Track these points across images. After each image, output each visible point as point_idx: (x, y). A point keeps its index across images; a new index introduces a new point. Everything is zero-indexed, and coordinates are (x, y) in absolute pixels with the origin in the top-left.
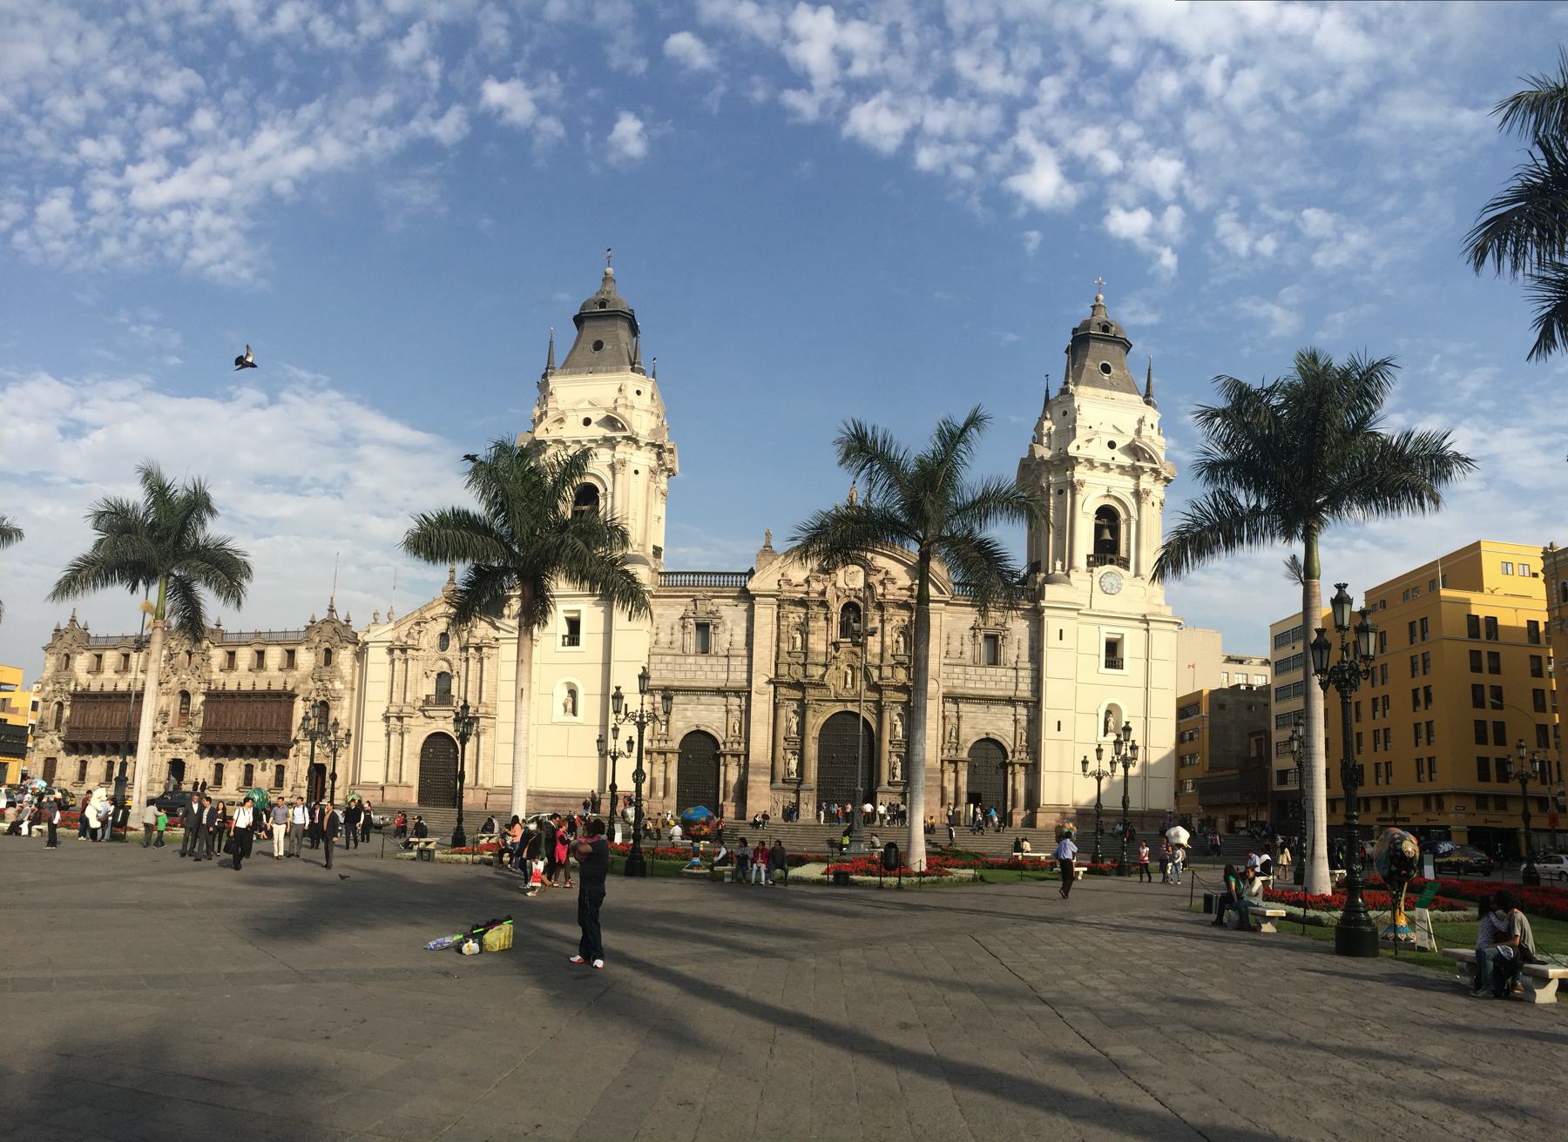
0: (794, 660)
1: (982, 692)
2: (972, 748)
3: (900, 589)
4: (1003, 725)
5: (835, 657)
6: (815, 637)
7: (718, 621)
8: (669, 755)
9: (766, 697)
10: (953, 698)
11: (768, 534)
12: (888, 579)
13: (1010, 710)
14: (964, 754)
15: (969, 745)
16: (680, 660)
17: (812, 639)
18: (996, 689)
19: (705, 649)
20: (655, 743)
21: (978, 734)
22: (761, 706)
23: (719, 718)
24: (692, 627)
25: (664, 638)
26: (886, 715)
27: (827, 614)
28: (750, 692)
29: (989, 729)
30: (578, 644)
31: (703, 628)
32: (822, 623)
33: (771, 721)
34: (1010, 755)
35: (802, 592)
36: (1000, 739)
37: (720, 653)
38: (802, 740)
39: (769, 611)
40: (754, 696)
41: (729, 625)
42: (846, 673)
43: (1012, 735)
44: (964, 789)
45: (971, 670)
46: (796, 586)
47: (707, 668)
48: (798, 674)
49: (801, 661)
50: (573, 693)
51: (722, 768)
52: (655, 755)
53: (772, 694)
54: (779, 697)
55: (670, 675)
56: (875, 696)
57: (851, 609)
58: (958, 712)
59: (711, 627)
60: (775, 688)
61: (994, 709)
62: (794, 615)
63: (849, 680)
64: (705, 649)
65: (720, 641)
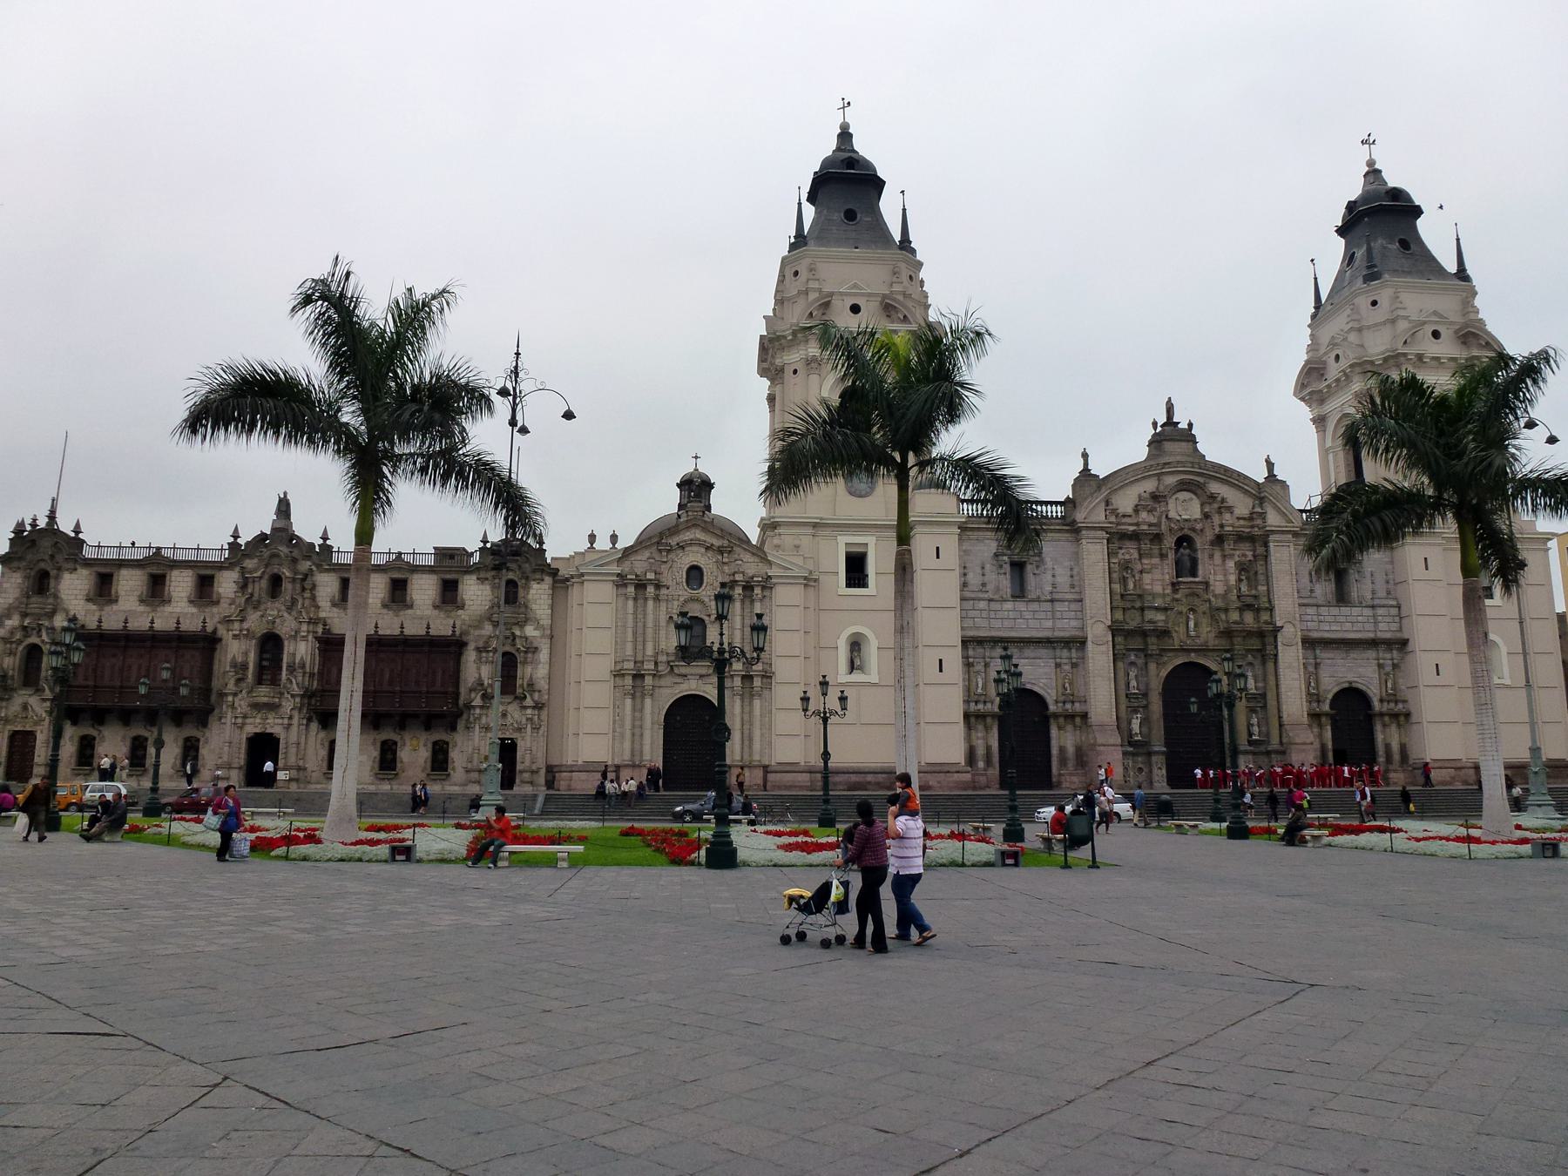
0: (1128, 605)
2: (1334, 697)
3: (1238, 518)
4: (1363, 672)
5: (1177, 600)
6: (1149, 576)
7: (1037, 558)
8: (989, 720)
9: (1103, 648)
10: (1309, 643)
11: (1085, 456)
12: (1224, 507)
13: (1371, 654)
14: (1326, 707)
15: (1330, 696)
16: (994, 606)
19: (1020, 592)
20: (972, 704)
21: (1337, 685)
22: (1099, 657)
23: (1046, 674)
24: (1007, 567)
25: (974, 579)
27: (1161, 549)
29: (1350, 677)
32: (1156, 561)
33: (1112, 675)
34: (1376, 705)
36: (1364, 688)
37: (1043, 598)
38: (1145, 695)
39: (1098, 547)
41: (1049, 564)
42: (1188, 617)
43: (1376, 682)
44: (1330, 745)
45: (1323, 610)
46: (1124, 516)
47: (1028, 615)
48: (1133, 622)
49: (1138, 604)
50: (856, 645)
51: (1054, 732)
52: (973, 720)
53: (1111, 643)
54: (1118, 647)
55: (984, 623)
56: (1223, 643)
57: (1184, 541)
58: (1315, 658)
59: (1029, 568)
60: (1113, 637)
61: (1354, 654)
62: (1123, 551)
63: (1192, 624)
64: (1020, 592)
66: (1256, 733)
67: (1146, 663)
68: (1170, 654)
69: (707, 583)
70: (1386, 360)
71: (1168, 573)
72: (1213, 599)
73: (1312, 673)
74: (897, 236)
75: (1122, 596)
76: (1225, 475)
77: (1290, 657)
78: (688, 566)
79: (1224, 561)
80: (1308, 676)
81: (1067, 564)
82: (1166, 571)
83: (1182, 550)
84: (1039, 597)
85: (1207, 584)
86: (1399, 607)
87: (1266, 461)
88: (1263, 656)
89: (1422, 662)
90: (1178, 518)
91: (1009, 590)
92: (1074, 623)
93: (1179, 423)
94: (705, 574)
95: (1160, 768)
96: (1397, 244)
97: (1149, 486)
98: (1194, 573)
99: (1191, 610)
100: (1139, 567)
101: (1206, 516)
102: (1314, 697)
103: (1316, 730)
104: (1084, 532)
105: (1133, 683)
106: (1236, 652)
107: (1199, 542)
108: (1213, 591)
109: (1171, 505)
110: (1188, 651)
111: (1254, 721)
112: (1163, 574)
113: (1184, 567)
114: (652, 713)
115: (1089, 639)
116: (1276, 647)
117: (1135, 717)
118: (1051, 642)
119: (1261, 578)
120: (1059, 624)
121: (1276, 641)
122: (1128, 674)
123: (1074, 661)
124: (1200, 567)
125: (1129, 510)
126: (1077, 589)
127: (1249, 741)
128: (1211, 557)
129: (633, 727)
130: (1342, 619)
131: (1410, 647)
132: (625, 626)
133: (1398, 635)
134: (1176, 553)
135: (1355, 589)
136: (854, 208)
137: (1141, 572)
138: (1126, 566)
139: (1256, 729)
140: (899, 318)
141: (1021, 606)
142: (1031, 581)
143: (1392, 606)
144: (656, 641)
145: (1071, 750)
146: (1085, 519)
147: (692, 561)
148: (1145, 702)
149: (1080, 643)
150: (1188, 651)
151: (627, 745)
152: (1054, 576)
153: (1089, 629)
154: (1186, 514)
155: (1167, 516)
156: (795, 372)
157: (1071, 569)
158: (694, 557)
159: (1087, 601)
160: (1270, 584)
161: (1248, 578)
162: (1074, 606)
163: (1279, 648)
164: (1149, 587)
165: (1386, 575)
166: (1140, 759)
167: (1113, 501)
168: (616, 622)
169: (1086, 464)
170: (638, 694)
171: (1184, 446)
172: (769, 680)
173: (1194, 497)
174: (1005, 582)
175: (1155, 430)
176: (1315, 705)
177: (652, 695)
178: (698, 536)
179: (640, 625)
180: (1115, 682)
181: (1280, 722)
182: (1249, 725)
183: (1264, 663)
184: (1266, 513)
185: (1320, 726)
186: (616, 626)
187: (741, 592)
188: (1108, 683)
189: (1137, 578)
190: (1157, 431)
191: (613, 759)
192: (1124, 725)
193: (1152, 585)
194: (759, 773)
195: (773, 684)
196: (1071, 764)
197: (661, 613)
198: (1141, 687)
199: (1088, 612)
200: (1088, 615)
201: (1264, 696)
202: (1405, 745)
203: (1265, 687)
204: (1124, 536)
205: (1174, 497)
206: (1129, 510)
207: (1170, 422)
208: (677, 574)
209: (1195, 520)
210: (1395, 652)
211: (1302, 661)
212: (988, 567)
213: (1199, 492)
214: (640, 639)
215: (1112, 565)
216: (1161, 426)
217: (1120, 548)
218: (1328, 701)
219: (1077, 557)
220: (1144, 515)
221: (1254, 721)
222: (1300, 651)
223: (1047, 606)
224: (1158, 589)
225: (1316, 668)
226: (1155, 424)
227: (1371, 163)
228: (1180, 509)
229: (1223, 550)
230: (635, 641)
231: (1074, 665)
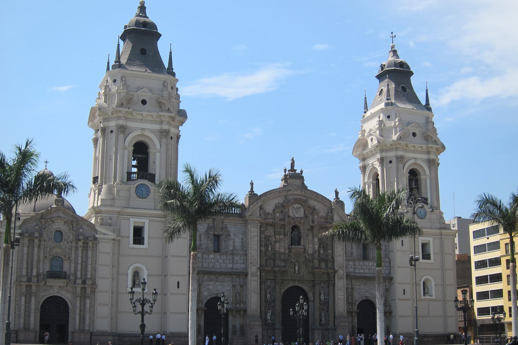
1: (363, 275)
9: (256, 278)
11: (252, 184)
14: (355, 308)
15: (357, 303)
16: (205, 256)
17: (277, 245)
18: (370, 273)
19: (217, 250)
24: (212, 237)
26: (317, 288)
28: (246, 275)
29: (367, 294)
30: (143, 244)
31: (217, 237)
32: (282, 237)
33: (259, 291)
35: (271, 219)
40: (249, 277)
41: (232, 236)
44: (356, 326)
45: (357, 263)
47: (220, 261)
51: (230, 318)
53: (259, 276)
57: (295, 228)
58: (352, 285)
59: (222, 238)
60: (260, 273)
63: (297, 268)
65: (228, 245)
66: (324, 320)
67: (275, 286)
68: (286, 282)
69: (65, 240)
70: (391, 145)
71: (287, 243)
72: (307, 256)
73: (350, 293)
74: (166, 65)
75: (265, 253)
76: (316, 197)
77: (341, 284)
78: (55, 230)
79: (313, 238)
80: (348, 293)
81: (240, 236)
82: (286, 242)
83: (294, 232)
84: (226, 252)
85: (305, 249)
86: (390, 263)
87: (335, 191)
88: (328, 284)
89: (398, 289)
90: (293, 216)
91: (212, 249)
92: (242, 266)
93: (296, 170)
94: (64, 235)
95: (279, 336)
96: (401, 89)
97: (281, 200)
98: (299, 244)
99: (296, 261)
100: (273, 239)
101: (306, 216)
102: (349, 302)
103: (350, 319)
104: (249, 222)
105: (268, 295)
106: (316, 282)
107: (302, 228)
108: (307, 252)
109: (291, 211)
110: (295, 281)
111: (323, 314)
112: (285, 243)
113: (296, 241)
114: (35, 304)
115: (249, 274)
116: (334, 280)
117: (269, 311)
118: (231, 275)
119: (330, 247)
120: (235, 266)
121: (334, 277)
122: (267, 291)
123: (242, 284)
124: (302, 240)
125: (271, 211)
126: (245, 249)
127: (320, 324)
128: (308, 236)
129: (25, 311)
130: (365, 267)
131: (393, 281)
132: (22, 260)
133: (389, 275)
134: (292, 233)
135: (371, 253)
136: (145, 48)
137: (275, 242)
138: (267, 238)
139: (323, 318)
140: (166, 109)
141: (218, 256)
142: (223, 244)
143: (387, 262)
144: (38, 268)
145: (238, 327)
146: (250, 215)
147: (58, 228)
148: (274, 305)
149: (245, 274)
150: (295, 281)
151: (22, 321)
152: (234, 242)
153: (249, 269)
154: (297, 215)
155: (288, 215)
156: (112, 132)
157: (242, 239)
158: (59, 225)
159: (249, 256)
160: (334, 250)
161: (323, 247)
162: (242, 258)
163: (336, 280)
164: (278, 249)
165: (385, 247)
166: (270, 332)
167: (264, 207)
168: (18, 258)
169: (252, 188)
170: (28, 295)
171: (298, 182)
172: (94, 290)
173: (301, 207)
174: (211, 244)
175: (285, 173)
176: (350, 307)
177: (35, 295)
178: (61, 215)
179: (30, 259)
180: (260, 295)
181: (334, 315)
182: (320, 316)
183: (329, 287)
184: (333, 216)
185: (352, 316)
186: (18, 260)
187: (82, 245)
188: (257, 295)
189: (273, 245)
190: (286, 174)
191: (14, 327)
192: (263, 316)
193: (280, 248)
194: (88, 336)
195: (96, 292)
196: (238, 333)
197: (41, 253)
198: (272, 297)
199: (249, 260)
200: (249, 262)
201: (328, 303)
202: (389, 326)
203: (328, 299)
204: (267, 224)
205: (292, 206)
206: (271, 211)
207: (292, 169)
208: (49, 234)
209: (301, 218)
210: (387, 283)
211: (345, 287)
212: (203, 236)
213: (304, 204)
214: (29, 267)
215: (262, 238)
216: (289, 171)
217: (266, 230)
218: (356, 306)
219: (245, 234)
220: (278, 215)
221: (323, 314)
222: (345, 282)
223: (230, 257)
224: (282, 250)
225: (352, 290)
226: (285, 170)
227: (393, 47)
228: (294, 212)
229: (313, 233)
230: (27, 268)
231: (242, 286)
